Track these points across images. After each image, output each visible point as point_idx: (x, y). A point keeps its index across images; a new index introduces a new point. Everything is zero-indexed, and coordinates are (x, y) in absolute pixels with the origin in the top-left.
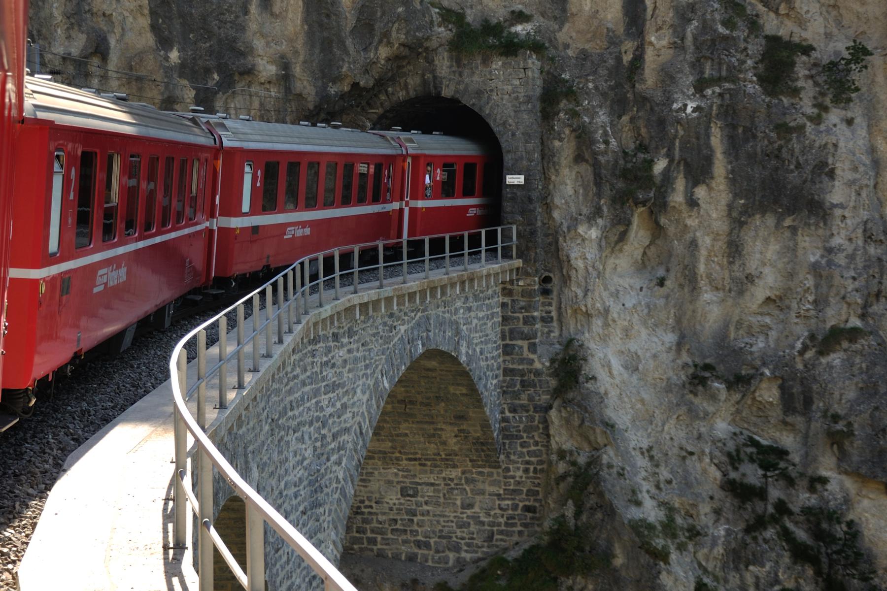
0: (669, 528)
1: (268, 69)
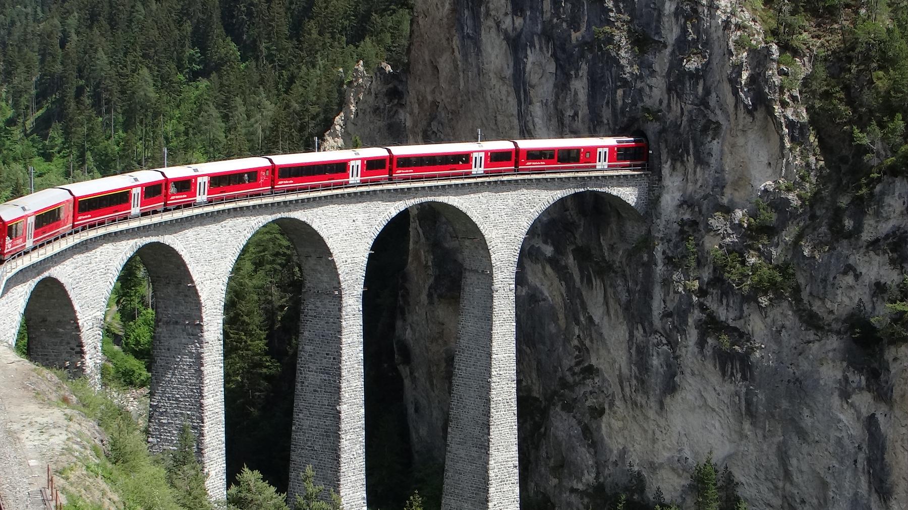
0: (662, 239)
1: (606, 122)
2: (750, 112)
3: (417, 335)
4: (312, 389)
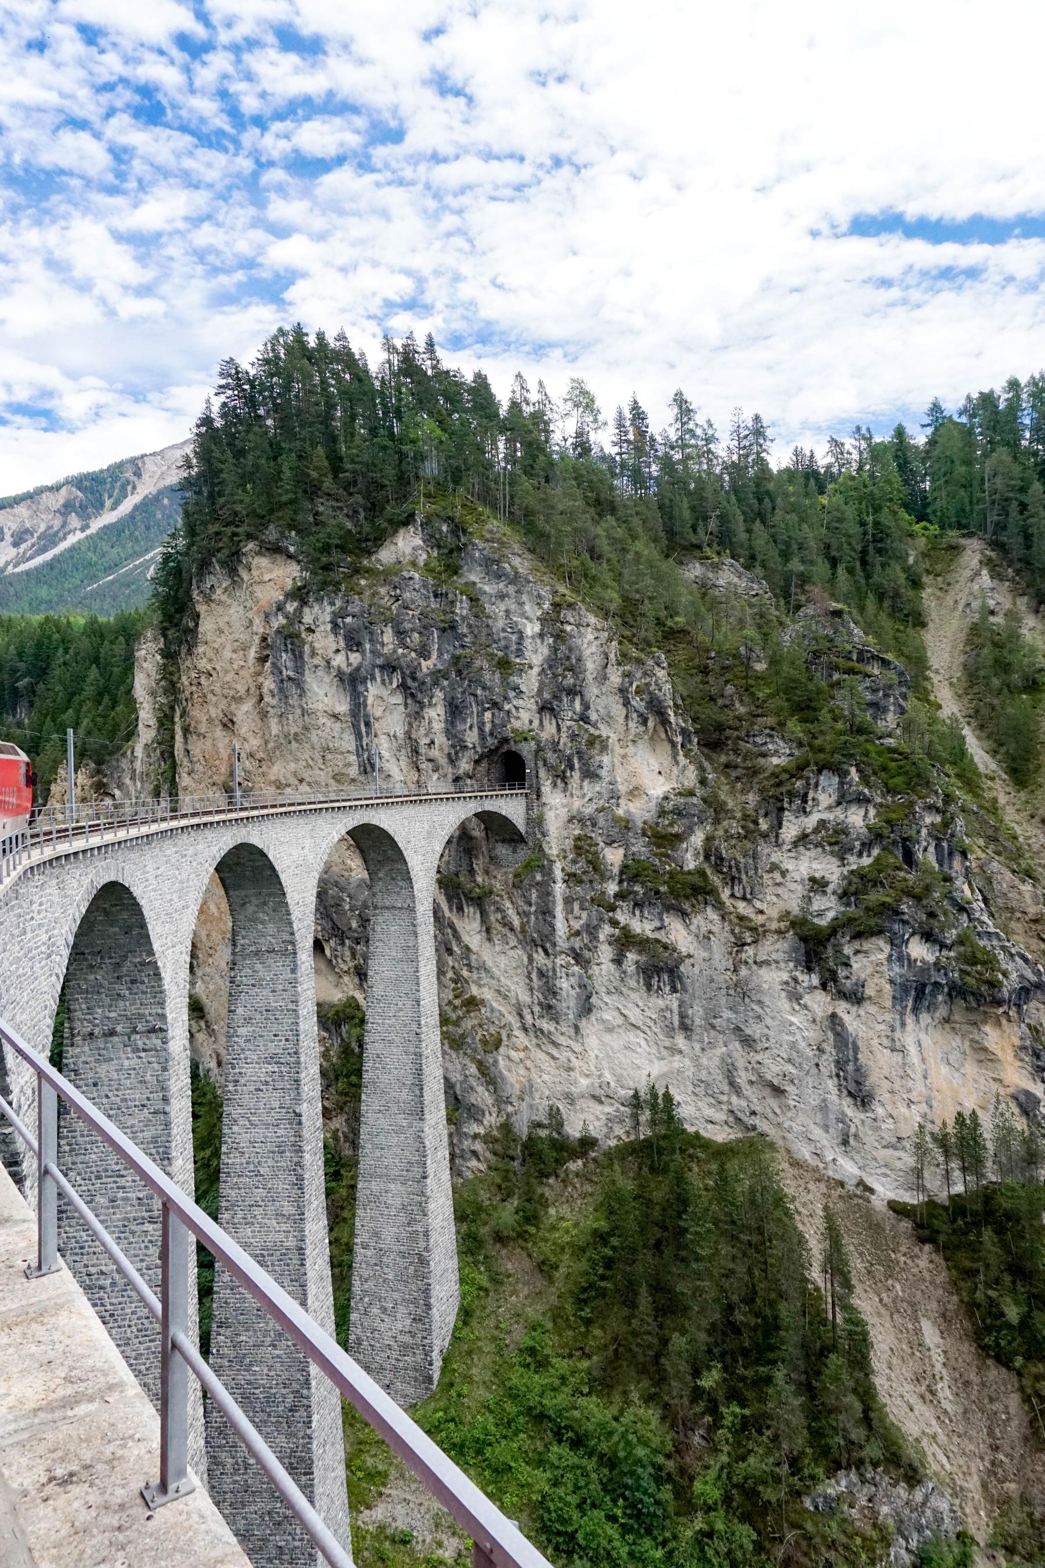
2: (644, 722)
3: (211, 987)
4: (252, 1088)
